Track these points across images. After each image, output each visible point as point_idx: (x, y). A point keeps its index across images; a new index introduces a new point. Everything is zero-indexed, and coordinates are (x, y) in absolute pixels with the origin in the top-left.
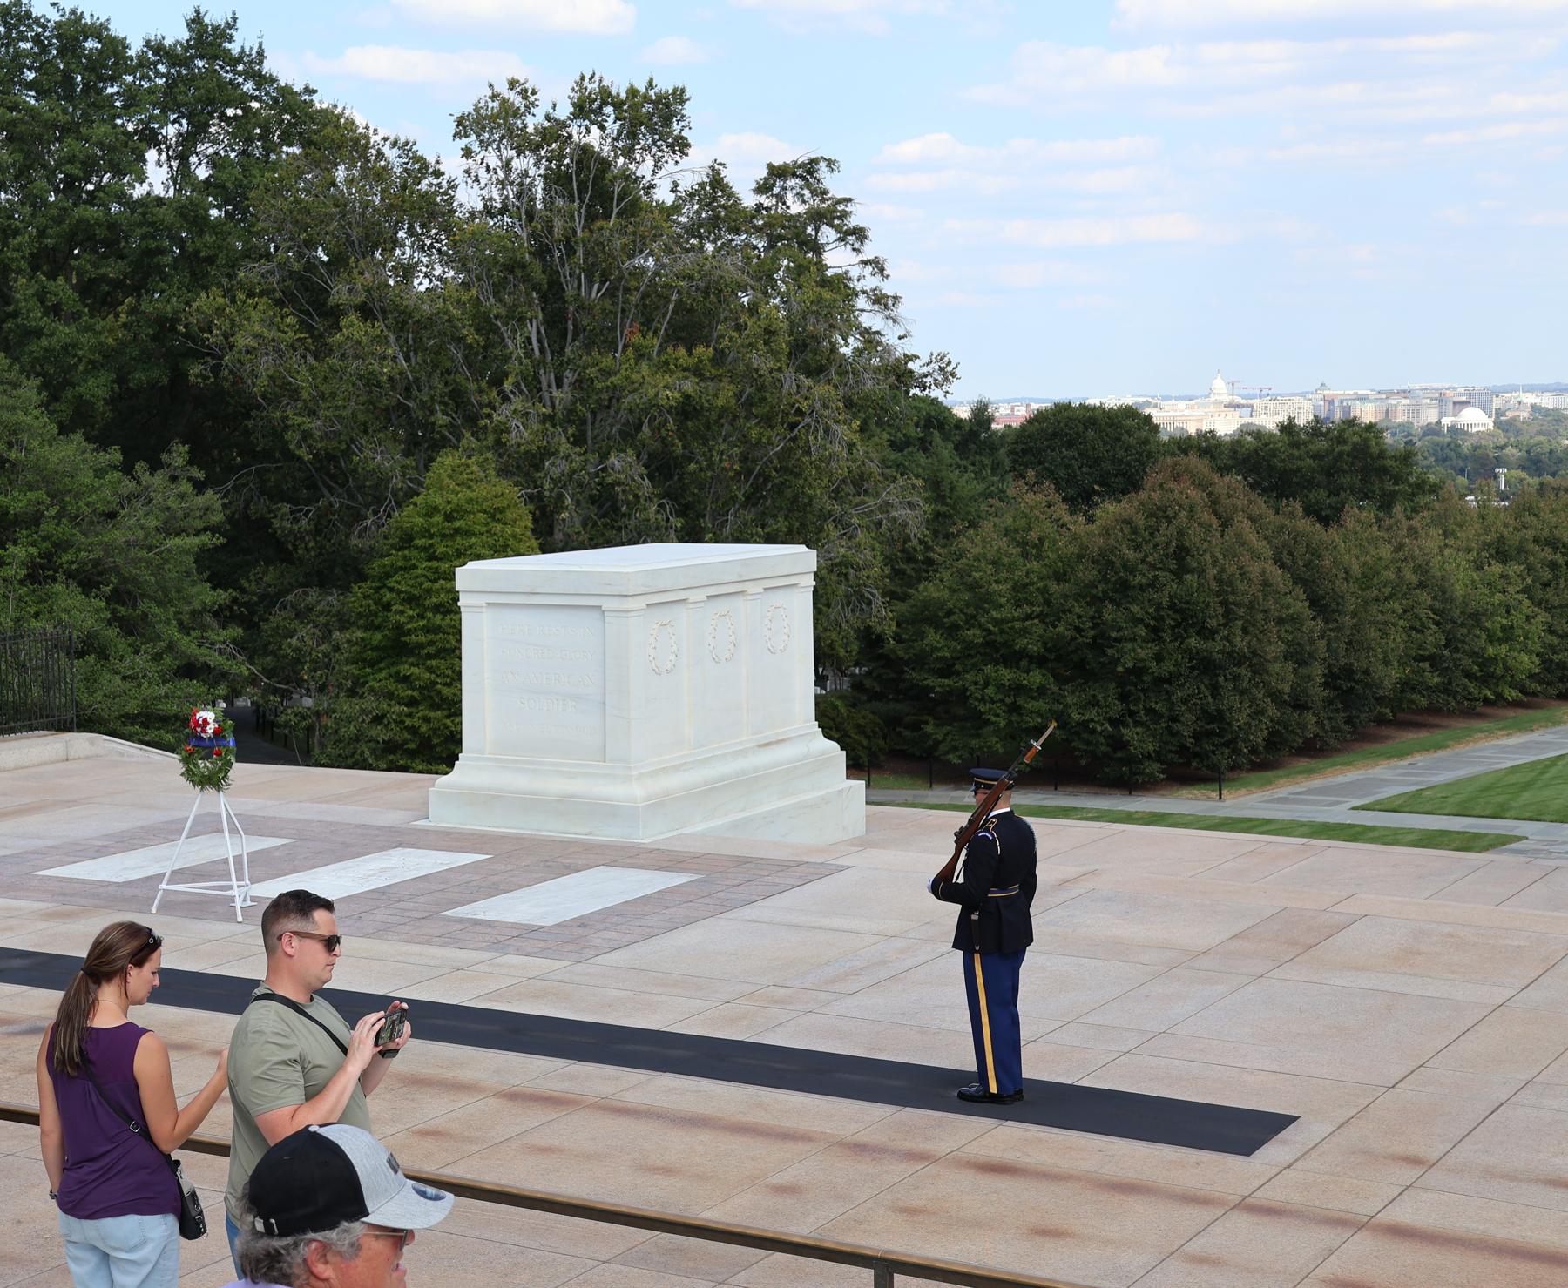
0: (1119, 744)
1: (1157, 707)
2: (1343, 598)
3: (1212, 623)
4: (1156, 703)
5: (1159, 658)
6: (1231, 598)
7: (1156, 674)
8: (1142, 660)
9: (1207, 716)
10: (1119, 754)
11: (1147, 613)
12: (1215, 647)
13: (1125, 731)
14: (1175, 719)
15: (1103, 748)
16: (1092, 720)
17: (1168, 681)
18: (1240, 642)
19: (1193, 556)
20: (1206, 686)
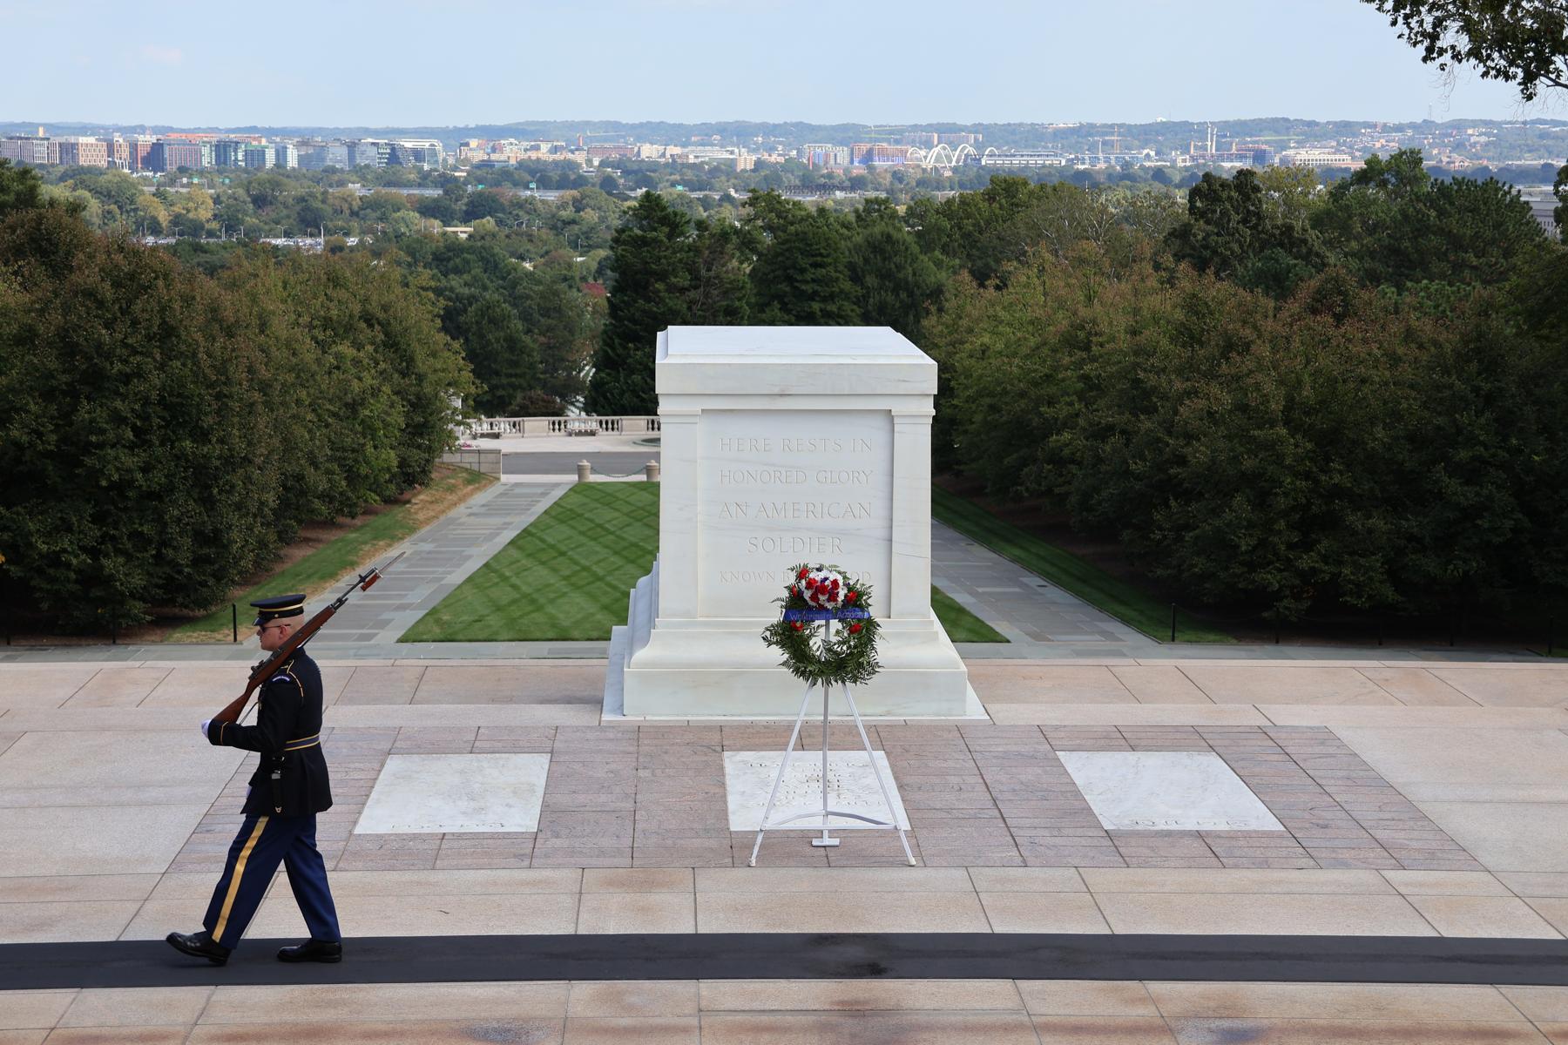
0: (92, 578)
1: (145, 529)
2: (271, 386)
3: (208, 421)
4: (141, 525)
5: (145, 469)
6: (225, 390)
7: (144, 488)
8: (129, 471)
9: (201, 538)
10: (96, 592)
11: (133, 410)
12: (214, 450)
13: (104, 561)
14: (164, 544)
15: (71, 587)
16: (65, 551)
17: (158, 497)
18: (240, 447)
19: (178, 337)
20: (195, 501)
